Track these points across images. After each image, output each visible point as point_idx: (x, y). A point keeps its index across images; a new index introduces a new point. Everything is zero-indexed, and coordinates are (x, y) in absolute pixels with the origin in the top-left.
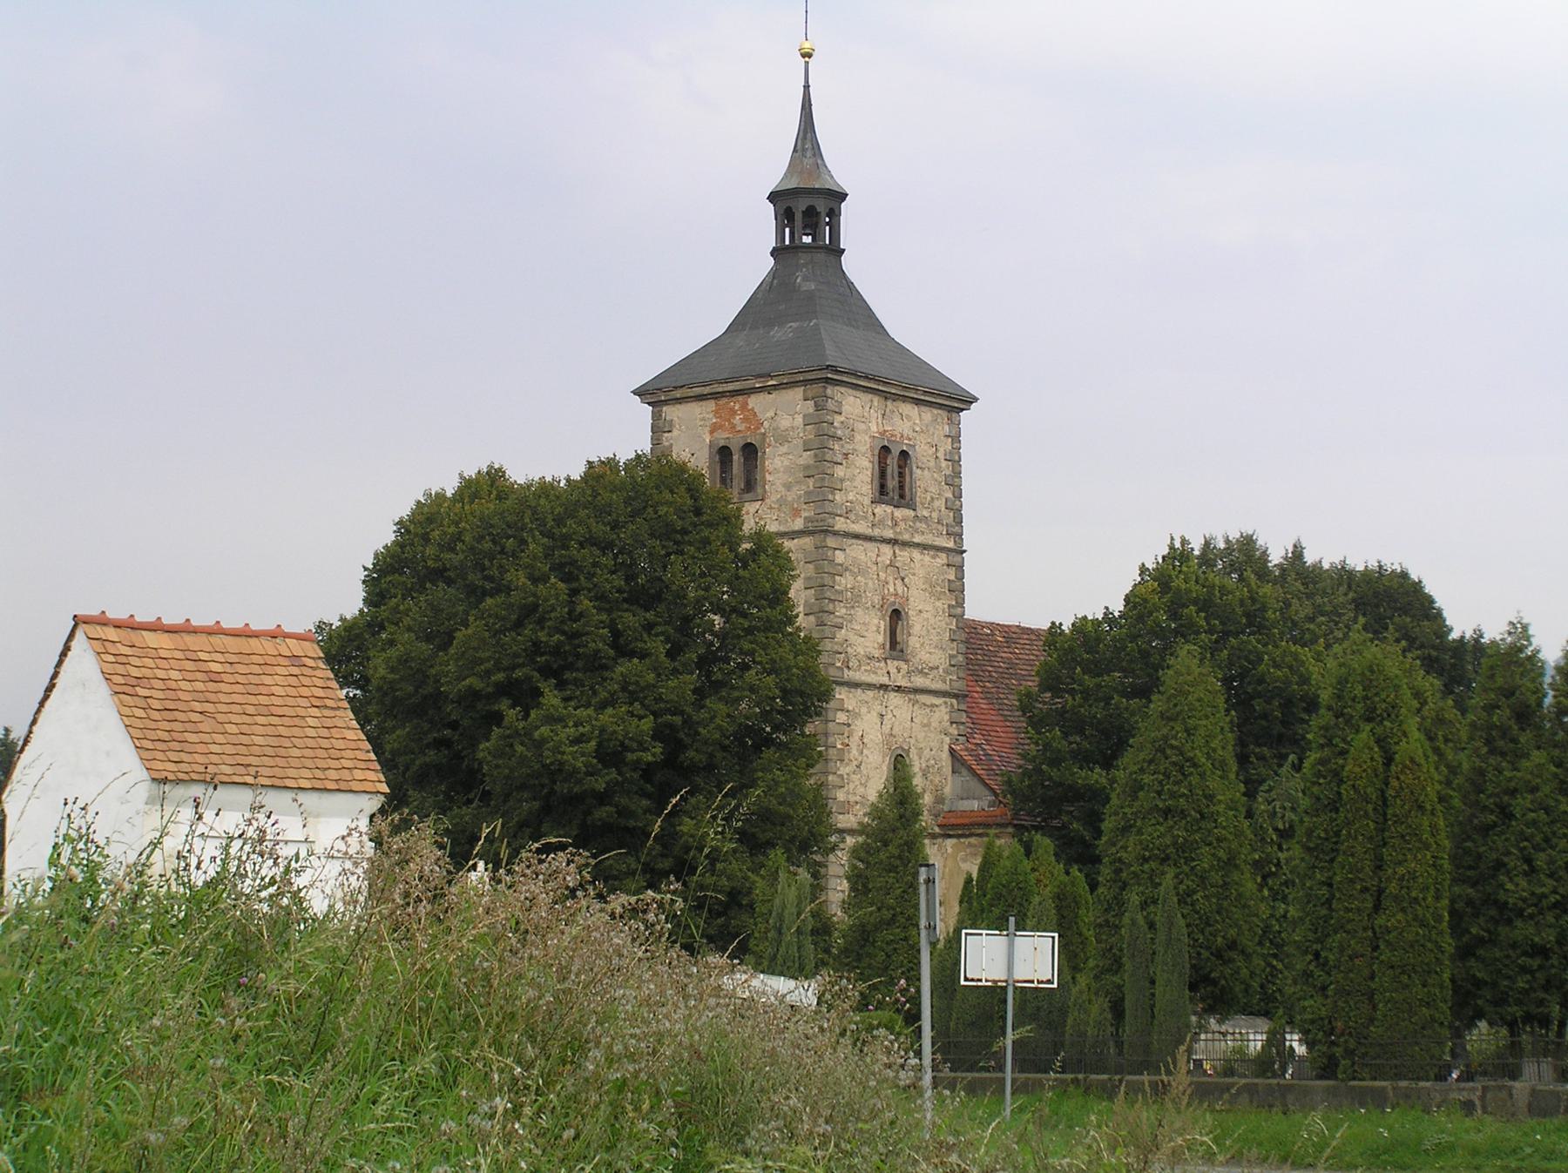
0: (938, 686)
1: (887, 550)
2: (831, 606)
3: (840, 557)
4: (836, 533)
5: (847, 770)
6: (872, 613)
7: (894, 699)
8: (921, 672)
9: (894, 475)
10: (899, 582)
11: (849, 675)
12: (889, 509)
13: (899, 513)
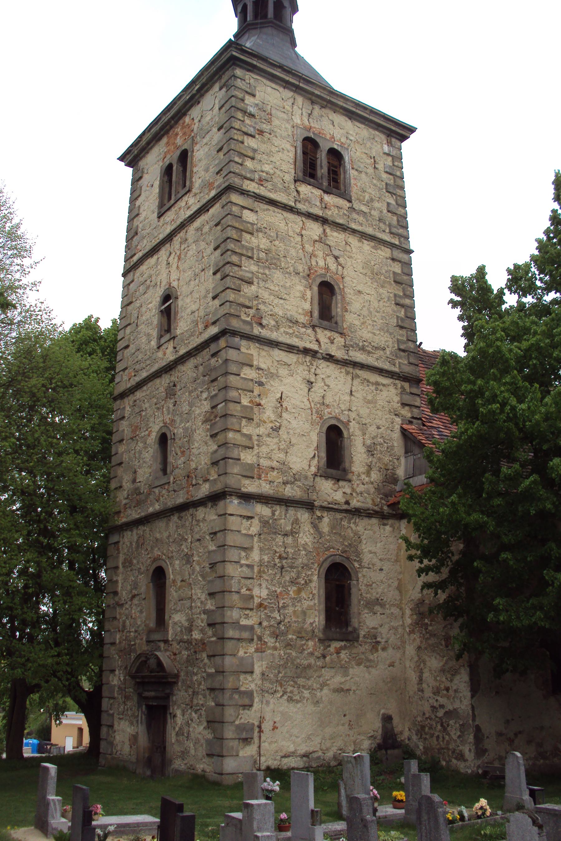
0: (387, 366)
1: (314, 230)
2: (235, 259)
3: (248, 216)
4: (243, 193)
5: (262, 430)
6: (296, 279)
7: (326, 369)
8: (363, 349)
9: (321, 165)
10: (331, 261)
11: (257, 330)
12: (318, 192)
13: (328, 198)
